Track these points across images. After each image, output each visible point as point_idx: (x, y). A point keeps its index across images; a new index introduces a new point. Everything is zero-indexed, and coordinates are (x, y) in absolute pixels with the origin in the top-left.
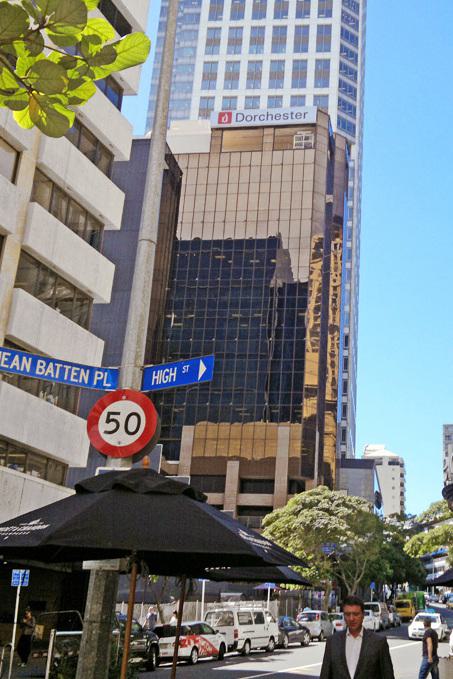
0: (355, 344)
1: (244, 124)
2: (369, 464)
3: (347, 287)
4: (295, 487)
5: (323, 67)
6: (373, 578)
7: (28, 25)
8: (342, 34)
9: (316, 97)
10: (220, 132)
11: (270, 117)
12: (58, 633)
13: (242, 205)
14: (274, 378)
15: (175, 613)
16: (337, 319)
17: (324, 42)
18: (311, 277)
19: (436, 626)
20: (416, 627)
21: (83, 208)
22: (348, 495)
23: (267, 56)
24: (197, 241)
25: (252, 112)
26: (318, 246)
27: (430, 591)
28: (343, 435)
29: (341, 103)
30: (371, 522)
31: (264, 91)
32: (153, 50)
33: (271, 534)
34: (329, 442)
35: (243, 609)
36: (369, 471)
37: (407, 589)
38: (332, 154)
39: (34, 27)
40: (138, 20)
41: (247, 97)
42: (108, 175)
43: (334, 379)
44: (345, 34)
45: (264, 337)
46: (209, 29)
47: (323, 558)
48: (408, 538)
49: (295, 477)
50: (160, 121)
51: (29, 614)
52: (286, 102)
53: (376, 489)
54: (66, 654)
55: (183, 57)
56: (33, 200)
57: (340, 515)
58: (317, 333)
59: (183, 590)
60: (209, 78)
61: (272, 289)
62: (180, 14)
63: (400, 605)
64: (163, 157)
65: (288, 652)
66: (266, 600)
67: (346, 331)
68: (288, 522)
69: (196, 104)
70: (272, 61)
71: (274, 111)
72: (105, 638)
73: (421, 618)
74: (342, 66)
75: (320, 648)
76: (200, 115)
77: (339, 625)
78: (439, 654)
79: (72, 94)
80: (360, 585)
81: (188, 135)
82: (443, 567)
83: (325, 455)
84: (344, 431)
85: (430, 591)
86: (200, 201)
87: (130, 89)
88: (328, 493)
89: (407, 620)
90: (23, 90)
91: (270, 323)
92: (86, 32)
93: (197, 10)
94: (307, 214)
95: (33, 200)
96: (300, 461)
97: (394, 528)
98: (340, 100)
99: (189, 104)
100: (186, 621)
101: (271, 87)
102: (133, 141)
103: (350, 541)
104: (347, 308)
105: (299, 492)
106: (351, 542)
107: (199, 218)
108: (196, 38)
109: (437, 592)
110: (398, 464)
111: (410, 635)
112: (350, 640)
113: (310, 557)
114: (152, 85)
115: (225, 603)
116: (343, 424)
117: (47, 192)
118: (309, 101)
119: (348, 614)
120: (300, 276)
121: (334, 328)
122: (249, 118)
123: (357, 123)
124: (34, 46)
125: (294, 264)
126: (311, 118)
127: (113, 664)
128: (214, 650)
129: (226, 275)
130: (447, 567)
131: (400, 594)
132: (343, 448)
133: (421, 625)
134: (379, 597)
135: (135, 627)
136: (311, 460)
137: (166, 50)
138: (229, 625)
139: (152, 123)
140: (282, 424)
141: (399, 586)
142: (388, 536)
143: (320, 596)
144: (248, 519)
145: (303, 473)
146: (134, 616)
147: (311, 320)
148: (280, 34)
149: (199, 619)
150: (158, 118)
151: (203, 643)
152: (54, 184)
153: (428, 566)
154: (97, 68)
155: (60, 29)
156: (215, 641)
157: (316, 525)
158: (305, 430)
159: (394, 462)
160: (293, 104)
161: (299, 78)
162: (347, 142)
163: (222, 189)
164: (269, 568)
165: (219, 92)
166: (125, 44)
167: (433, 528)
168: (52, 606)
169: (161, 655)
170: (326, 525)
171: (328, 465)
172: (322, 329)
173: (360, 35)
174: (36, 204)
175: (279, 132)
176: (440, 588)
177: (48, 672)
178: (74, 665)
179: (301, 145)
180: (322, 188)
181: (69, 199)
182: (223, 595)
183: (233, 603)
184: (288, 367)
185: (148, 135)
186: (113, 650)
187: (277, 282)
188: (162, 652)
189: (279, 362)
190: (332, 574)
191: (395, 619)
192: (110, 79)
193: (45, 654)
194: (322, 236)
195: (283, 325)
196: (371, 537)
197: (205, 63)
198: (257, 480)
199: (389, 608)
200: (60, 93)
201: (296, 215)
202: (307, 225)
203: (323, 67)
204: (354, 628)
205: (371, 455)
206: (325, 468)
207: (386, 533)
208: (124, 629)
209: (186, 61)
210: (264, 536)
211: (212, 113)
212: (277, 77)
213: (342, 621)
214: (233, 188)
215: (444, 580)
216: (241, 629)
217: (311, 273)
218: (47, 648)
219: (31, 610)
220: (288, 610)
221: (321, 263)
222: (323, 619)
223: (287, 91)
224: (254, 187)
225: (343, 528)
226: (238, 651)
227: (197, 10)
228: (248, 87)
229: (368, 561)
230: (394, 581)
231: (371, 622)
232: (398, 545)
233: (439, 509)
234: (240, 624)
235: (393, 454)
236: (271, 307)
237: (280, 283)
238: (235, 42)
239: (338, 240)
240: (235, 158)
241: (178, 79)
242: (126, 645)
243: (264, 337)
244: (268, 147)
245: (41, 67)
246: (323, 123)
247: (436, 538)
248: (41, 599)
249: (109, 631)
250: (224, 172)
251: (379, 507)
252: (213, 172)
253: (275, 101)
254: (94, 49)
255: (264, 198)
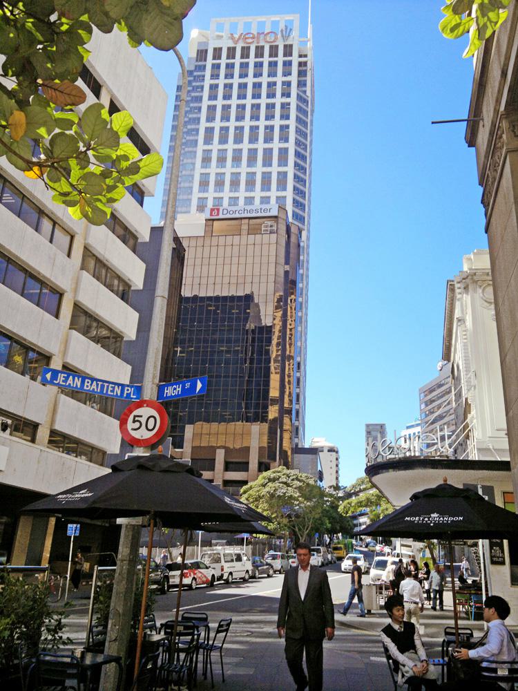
0: (305, 368)
1: (228, 216)
2: (314, 451)
3: (299, 329)
4: (263, 467)
5: (282, 177)
6: (317, 530)
7: (79, 147)
8: (297, 120)
9: (278, 198)
10: (211, 222)
11: (246, 211)
12: (99, 568)
13: (227, 273)
14: (249, 392)
15: (181, 554)
16: (292, 351)
17: (283, 160)
18: (275, 322)
19: (361, 563)
20: (346, 564)
21: (117, 275)
22: (300, 473)
23: (244, 169)
24: (196, 297)
25: (234, 208)
26: (279, 300)
27: (356, 539)
28: (296, 431)
29: (295, 202)
30: (315, 491)
31: (242, 194)
32: (165, 165)
33: (247, 499)
34: (286, 436)
35: (227, 552)
36: (314, 456)
37: (340, 538)
38: (289, 237)
39: (83, 149)
40: (155, 145)
41: (230, 198)
42: (134, 251)
43: (290, 393)
44: (297, 154)
45: (242, 364)
46: (203, 150)
47: (282, 516)
48: (341, 502)
49: (263, 460)
50: (170, 214)
51: (80, 555)
52: (257, 201)
53: (319, 468)
54: (105, 582)
55: (185, 170)
56: (82, 268)
57: (294, 486)
58: (279, 361)
59: (186, 538)
60: (204, 184)
61: (247, 330)
62: (184, 141)
63: (336, 549)
64: (172, 239)
65: (259, 581)
66: (243, 545)
67: (298, 359)
68: (258, 491)
69: (194, 203)
70: (247, 173)
71: (249, 208)
72: (132, 572)
73: (350, 558)
74: (296, 176)
75: (280, 578)
76: (197, 210)
77: (293, 562)
78: (363, 582)
79: (109, 195)
80: (308, 535)
81: (189, 224)
82: (366, 522)
83: (284, 445)
84: (297, 429)
85: (356, 539)
86: (198, 269)
87: (149, 192)
88: (286, 471)
89: (341, 559)
90: (76, 193)
91: (246, 354)
92: (119, 153)
93: (196, 138)
94: (272, 279)
95: (82, 268)
96: (267, 449)
97: (331, 495)
98: (294, 199)
99: (190, 203)
100: (188, 559)
101: (246, 191)
102: (152, 228)
103: (301, 505)
104: (299, 344)
105: (266, 471)
106: (302, 505)
107: (197, 281)
108: (195, 157)
109: (361, 539)
110: (334, 451)
111: (343, 570)
112: (301, 573)
113: (273, 516)
114: (164, 190)
115: (215, 548)
116: (297, 423)
117: (92, 263)
118: (273, 201)
119: (299, 555)
120: (267, 321)
121: (290, 357)
122: (231, 212)
123: (306, 215)
124: (83, 162)
125: (262, 313)
126: (274, 212)
127: (138, 589)
128: (207, 580)
129: (215, 320)
130: (368, 522)
131: (336, 541)
132: (296, 440)
133: (350, 562)
134: (321, 543)
135: (153, 564)
136: (274, 450)
137: (174, 165)
138: (217, 562)
139: (164, 215)
140: (254, 423)
141: (335, 535)
142: (328, 501)
143: (280, 542)
144: (231, 489)
145: (269, 457)
146: (152, 556)
147: (274, 351)
148: (253, 154)
149: (197, 558)
150: (169, 212)
151: (200, 575)
152: (97, 258)
153: (355, 522)
154: (126, 178)
155: (101, 151)
156: (208, 574)
157: (278, 493)
158: (270, 428)
159: (331, 450)
160: (262, 203)
161: (266, 185)
162: (299, 229)
163: (213, 261)
164: (247, 523)
165: (211, 194)
166: (146, 162)
167: (358, 495)
168: (95, 549)
169: (171, 583)
170: (285, 494)
171: (286, 452)
172: (282, 357)
173: (308, 155)
174: (84, 272)
175: (252, 222)
176: (363, 537)
177: (92, 595)
178: (111, 590)
179: (267, 231)
180: (282, 260)
181: (107, 268)
182: (214, 542)
183: (220, 548)
184: (258, 384)
185: (162, 224)
186: (138, 579)
187: (251, 325)
188: (172, 581)
189: (252, 381)
190: (289, 528)
191: (332, 559)
192: (135, 185)
193: (90, 583)
194: (282, 294)
195: (255, 355)
196: (316, 502)
197: (201, 174)
198: (237, 462)
199: (328, 551)
200: (101, 195)
201: (264, 279)
202: (271, 287)
203: (282, 177)
204: (304, 564)
205: (316, 445)
206: (284, 454)
207: (326, 499)
208: (145, 565)
209: (188, 173)
210: (244, 501)
211: (206, 209)
212: (251, 184)
213: (296, 560)
214: (220, 261)
215: (367, 532)
216: (226, 566)
217: (274, 319)
218: (92, 578)
219: (81, 552)
220: (258, 551)
221: (281, 312)
222: (282, 558)
223: (258, 193)
224: (235, 260)
225: (296, 496)
226: (224, 580)
227: (196, 138)
228: (231, 191)
229: (314, 518)
230: (332, 532)
231: (316, 560)
232: (335, 507)
233: (363, 482)
234: (225, 562)
235: (331, 445)
236: (247, 343)
237: (253, 326)
238: (222, 160)
239: (293, 297)
240: (222, 239)
241: (182, 185)
242: (146, 576)
243: (242, 364)
244: (244, 232)
245: (87, 177)
246: (282, 215)
247: (361, 502)
248: (88, 545)
249: (135, 567)
250: (214, 249)
251: (321, 481)
252: (207, 249)
253: (250, 200)
254: (124, 164)
255: (242, 268)
